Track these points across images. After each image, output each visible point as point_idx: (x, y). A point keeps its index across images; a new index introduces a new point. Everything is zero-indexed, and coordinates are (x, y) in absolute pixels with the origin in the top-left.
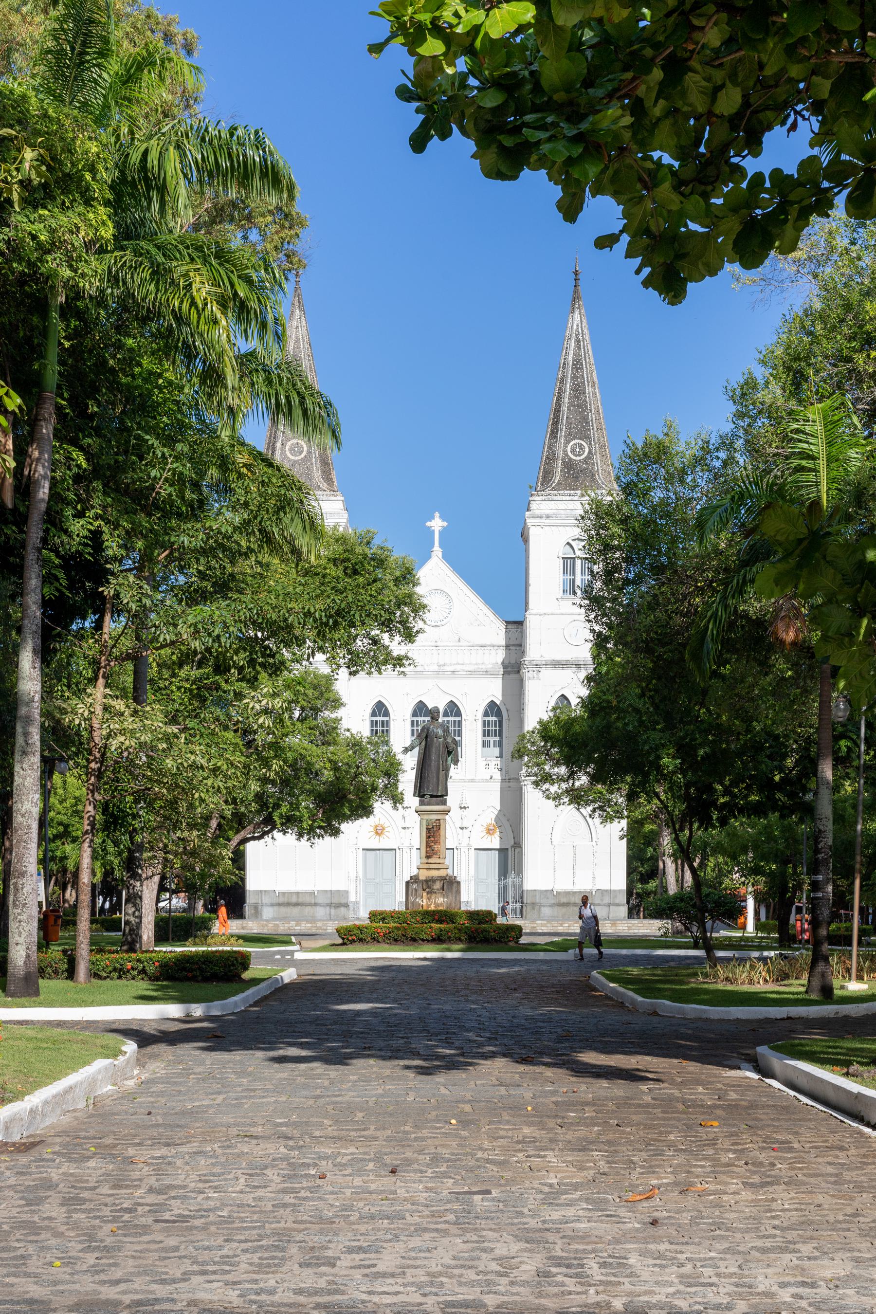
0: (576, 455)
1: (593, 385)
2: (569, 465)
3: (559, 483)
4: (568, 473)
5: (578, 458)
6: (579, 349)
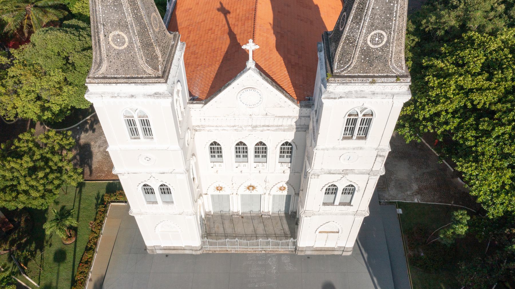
0: (375, 44)
2: (367, 53)
3: (355, 68)
4: (365, 59)
5: (376, 47)
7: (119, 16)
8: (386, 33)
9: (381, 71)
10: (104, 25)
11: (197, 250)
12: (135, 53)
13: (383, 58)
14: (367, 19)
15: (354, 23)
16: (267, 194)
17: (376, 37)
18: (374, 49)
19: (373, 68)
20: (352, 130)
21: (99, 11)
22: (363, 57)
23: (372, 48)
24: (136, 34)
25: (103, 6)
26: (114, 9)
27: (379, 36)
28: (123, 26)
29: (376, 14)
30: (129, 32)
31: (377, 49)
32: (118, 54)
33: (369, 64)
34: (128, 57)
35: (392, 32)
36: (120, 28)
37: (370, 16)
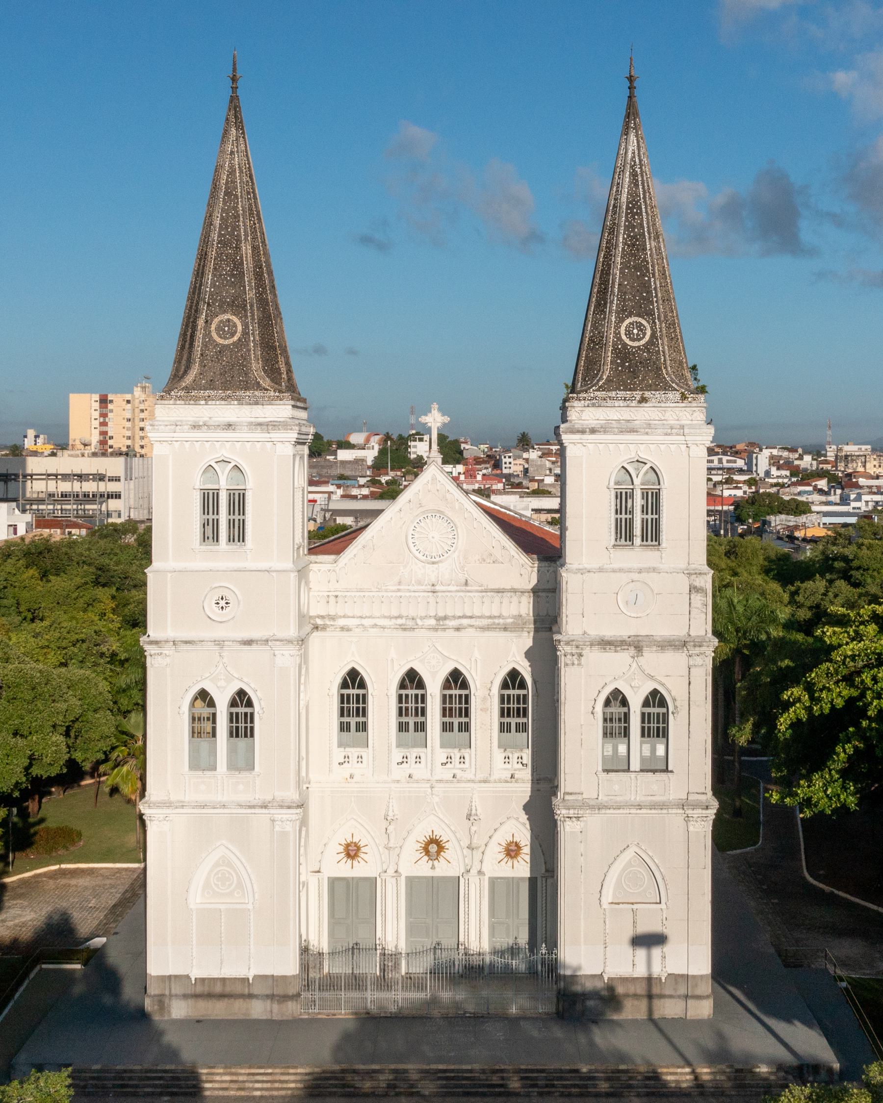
0: (633, 340)
1: (657, 237)
2: (623, 354)
3: (609, 380)
5: (636, 344)
6: (637, 186)
7: (235, 291)
8: (648, 322)
9: (653, 387)
10: (209, 304)
11: (285, 998)
12: (249, 350)
13: (652, 363)
14: (613, 300)
15: (598, 314)
16: (474, 871)
17: (634, 329)
18: (635, 347)
19: (639, 381)
20: (630, 537)
21: (207, 283)
22: (619, 361)
23: (631, 347)
24: (256, 321)
25: (214, 275)
26: (230, 280)
27: (637, 327)
28: (238, 306)
29: (625, 293)
30: (246, 317)
31: (639, 347)
32: (220, 352)
33: (631, 374)
34: (236, 357)
35: (657, 321)
36: (233, 309)
37: (618, 295)
